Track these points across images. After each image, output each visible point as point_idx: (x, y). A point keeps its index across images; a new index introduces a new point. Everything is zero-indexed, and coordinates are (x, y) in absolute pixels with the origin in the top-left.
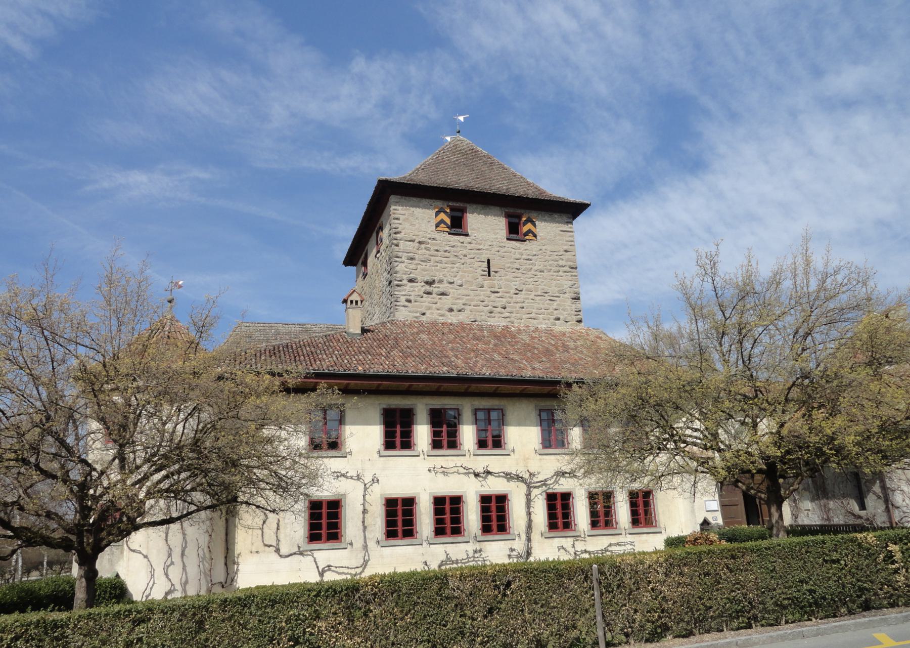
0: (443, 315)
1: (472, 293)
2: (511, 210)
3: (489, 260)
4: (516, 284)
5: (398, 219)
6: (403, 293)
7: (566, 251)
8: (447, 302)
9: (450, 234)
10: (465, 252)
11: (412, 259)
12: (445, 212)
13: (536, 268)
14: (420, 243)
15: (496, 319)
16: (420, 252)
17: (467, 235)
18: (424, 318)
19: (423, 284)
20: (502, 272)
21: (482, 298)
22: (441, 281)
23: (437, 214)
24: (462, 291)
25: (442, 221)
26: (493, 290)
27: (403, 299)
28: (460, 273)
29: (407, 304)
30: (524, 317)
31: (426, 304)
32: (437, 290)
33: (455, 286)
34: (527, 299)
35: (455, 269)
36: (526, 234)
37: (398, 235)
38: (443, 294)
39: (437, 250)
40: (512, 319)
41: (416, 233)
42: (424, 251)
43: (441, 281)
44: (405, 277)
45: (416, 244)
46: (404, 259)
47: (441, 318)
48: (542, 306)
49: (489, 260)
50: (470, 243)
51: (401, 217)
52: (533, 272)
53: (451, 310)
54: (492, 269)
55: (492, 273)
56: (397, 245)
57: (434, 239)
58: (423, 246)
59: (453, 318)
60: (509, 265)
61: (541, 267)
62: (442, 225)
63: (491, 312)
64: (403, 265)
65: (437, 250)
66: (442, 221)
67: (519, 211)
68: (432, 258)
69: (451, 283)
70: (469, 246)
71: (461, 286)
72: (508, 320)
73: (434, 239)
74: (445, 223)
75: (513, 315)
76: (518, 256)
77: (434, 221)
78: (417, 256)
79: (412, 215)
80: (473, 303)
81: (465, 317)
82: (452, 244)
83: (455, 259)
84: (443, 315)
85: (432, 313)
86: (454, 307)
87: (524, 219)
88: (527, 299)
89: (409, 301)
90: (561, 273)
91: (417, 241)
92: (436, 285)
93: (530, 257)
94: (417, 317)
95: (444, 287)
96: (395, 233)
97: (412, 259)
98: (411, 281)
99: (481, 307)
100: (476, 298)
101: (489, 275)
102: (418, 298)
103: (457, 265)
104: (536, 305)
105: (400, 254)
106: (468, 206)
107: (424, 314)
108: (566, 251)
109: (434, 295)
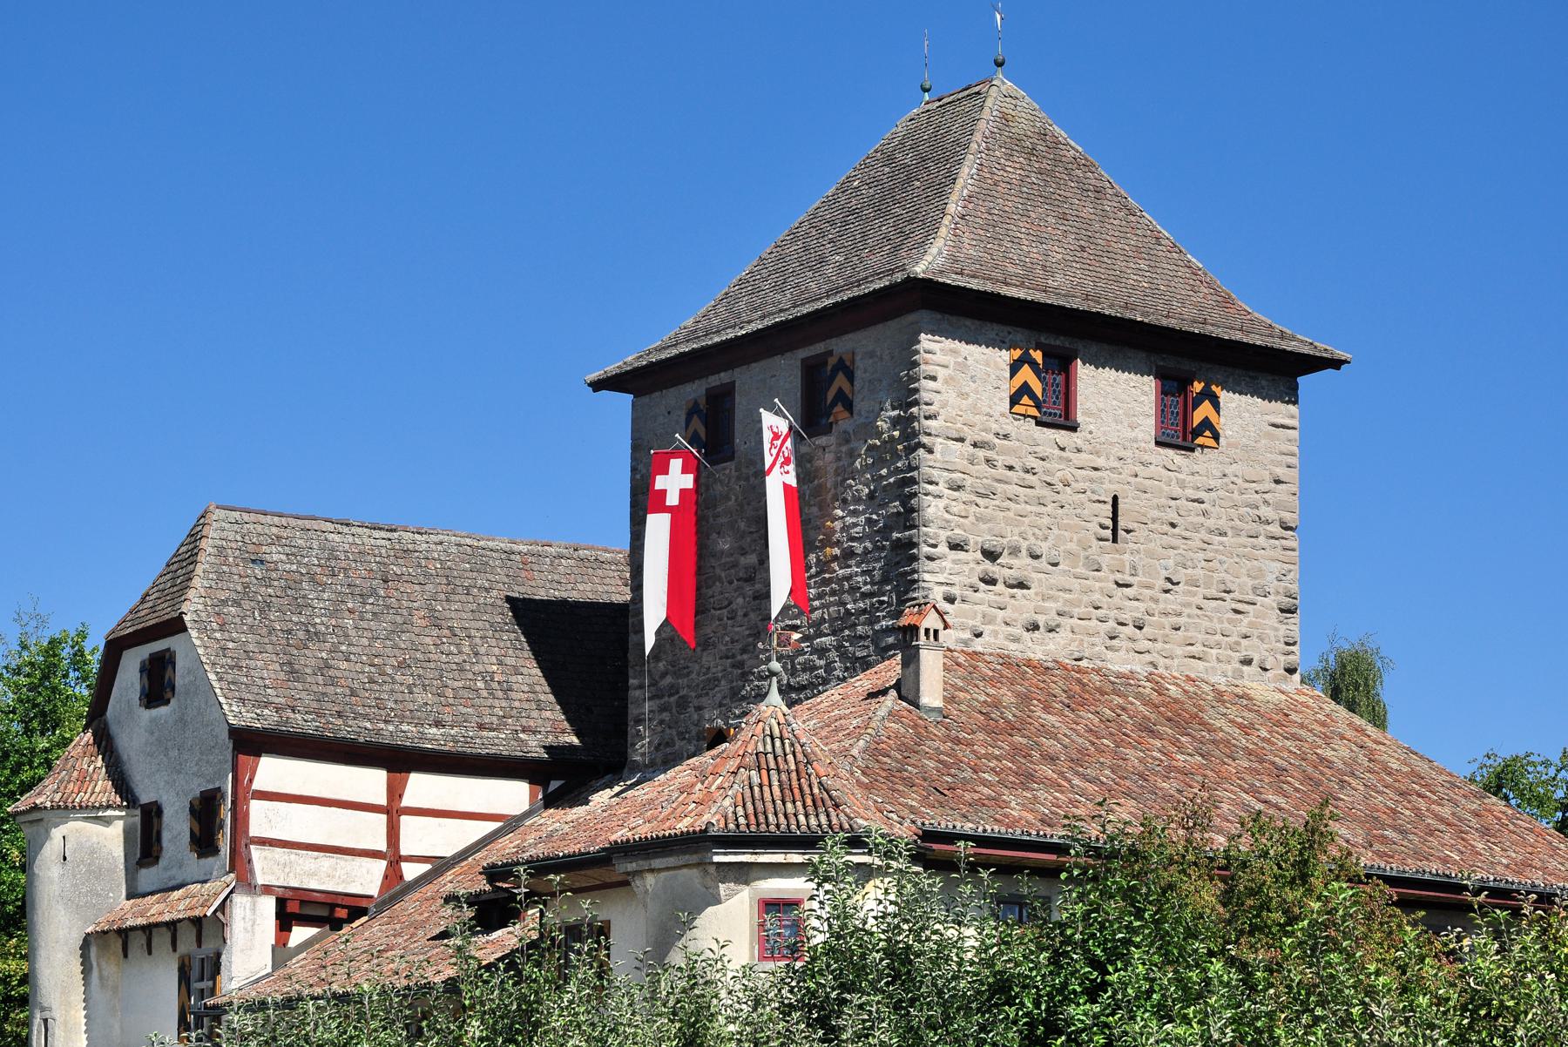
0: (1016, 640)
2: (1171, 363)
3: (1115, 498)
5: (934, 378)
8: (1024, 605)
9: (1039, 423)
12: (1033, 364)
13: (1211, 523)
17: (1074, 429)
18: (978, 646)
19: (979, 555)
20: (1141, 533)
23: (1015, 368)
24: (1057, 578)
25: (1025, 389)
26: (1118, 577)
28: (1056, 531)
31: (984, 608)
32: (1007, 572)
33: (1042, 564)
35: (1046, 521)
36: (1197, 432)
38: (1022, 585)
39: (1011, 468)
42: (984, 467)
43: (1015, 551)
49: (1115, 498)
51: (941, 373)
54: (1122, 523)
55: (1121, 533)
56: (931, 451)
57: (1006, 436)
58: (981, 453)
64: (941, 503)
65: (1011, 468)
66: (1025, 389)
67: (1187, 366)
68: (1000, 487)
69: (1036, 557)
71: (1055, 565)
73: (1006, 436)
74: (1032, 396)
76: (1177, 492)
77: (1007, 388)
78: (969, 481)
79: (962, 367)
80: (1076, 611)
94: (966, 643)
95: (1020, 566)
98: (955, 546)
99: (1094, 622)
100: (1085, 598)
101: (1115, 540)
102: (969, 593)
103: (1050, 508)
106: (1080, 345)
107: (978, 635)
109: (1000, 587)
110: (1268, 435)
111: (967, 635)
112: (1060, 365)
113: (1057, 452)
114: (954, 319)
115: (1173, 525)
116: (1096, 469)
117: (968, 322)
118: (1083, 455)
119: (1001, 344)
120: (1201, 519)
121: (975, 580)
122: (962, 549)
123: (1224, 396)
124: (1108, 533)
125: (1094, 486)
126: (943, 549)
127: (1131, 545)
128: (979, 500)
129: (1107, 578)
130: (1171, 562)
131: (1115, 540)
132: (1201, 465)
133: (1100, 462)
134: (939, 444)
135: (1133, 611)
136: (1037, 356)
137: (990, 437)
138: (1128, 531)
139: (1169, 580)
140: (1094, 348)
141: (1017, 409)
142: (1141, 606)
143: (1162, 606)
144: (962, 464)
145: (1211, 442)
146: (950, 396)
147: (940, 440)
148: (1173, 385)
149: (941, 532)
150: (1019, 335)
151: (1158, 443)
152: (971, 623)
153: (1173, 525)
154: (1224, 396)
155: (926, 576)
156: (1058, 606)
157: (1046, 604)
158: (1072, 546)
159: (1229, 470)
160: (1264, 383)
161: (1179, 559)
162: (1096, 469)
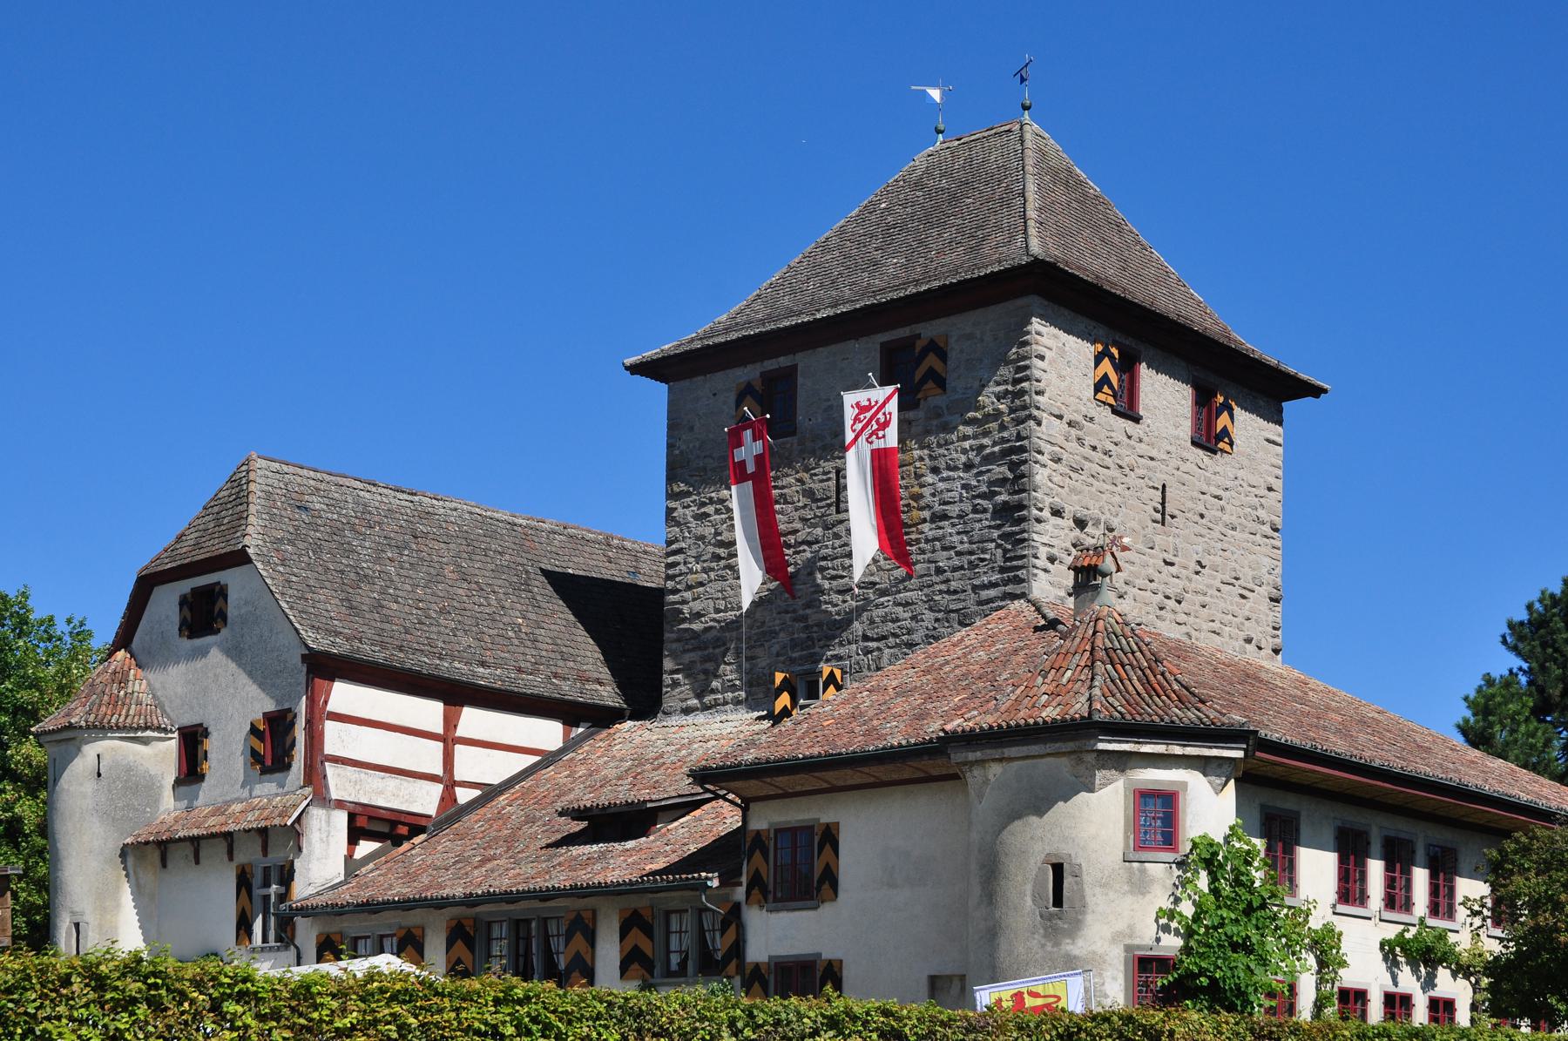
5: (1042, 358)
9: (1115, 412)
12: (1112, 357)
13: (1226, 518)
17: (1137, 419)
23: (1098, 360)
26: (1166, 556)
35: (1117, 499)
36: (1219, 438)
39: (1094, 448)
43: (1097, 523)
44: (1048, 500)
51: (1048, 354)
54: (1168, 510)
58: (1073, 432)
63: (1161, 609)
64: (1046, 472)
66: (1105, 380)
68: (1087, 465)
72: (1183, 629)
74: (1111, 387)
76: (1205, 488)
78: (1065, 456)
79: (1062, 352)
87: (1221, 399)
96: (1037, 393)
98: (1057, 513)
99: (1149, 594)
103: (1120, 488)
108: (1270, 489)
115: (1202, 516)
116: (1152, 459)
117: (1066, 312)
118: (1143, 445)
120: (1219, 514)
123: (1237, 411)
124: (1159, 516)
126: (1046, 514)
130: (1200, 549)
133: (1154, 453)
135: (1175, 587)
136: (1115, 351)
137: (1079, 418)
138: (1173, 517)
139: (1199, 563)
141: (1100, 396)
145: (1227, 448)
148: (1203, 399)
150: (1101, 331)
151: (1194, 443)
153: (1202, 516)
154: (1237, 411)
155: (1035, 537)
159: (1240, 474)
162: (1152, 459)
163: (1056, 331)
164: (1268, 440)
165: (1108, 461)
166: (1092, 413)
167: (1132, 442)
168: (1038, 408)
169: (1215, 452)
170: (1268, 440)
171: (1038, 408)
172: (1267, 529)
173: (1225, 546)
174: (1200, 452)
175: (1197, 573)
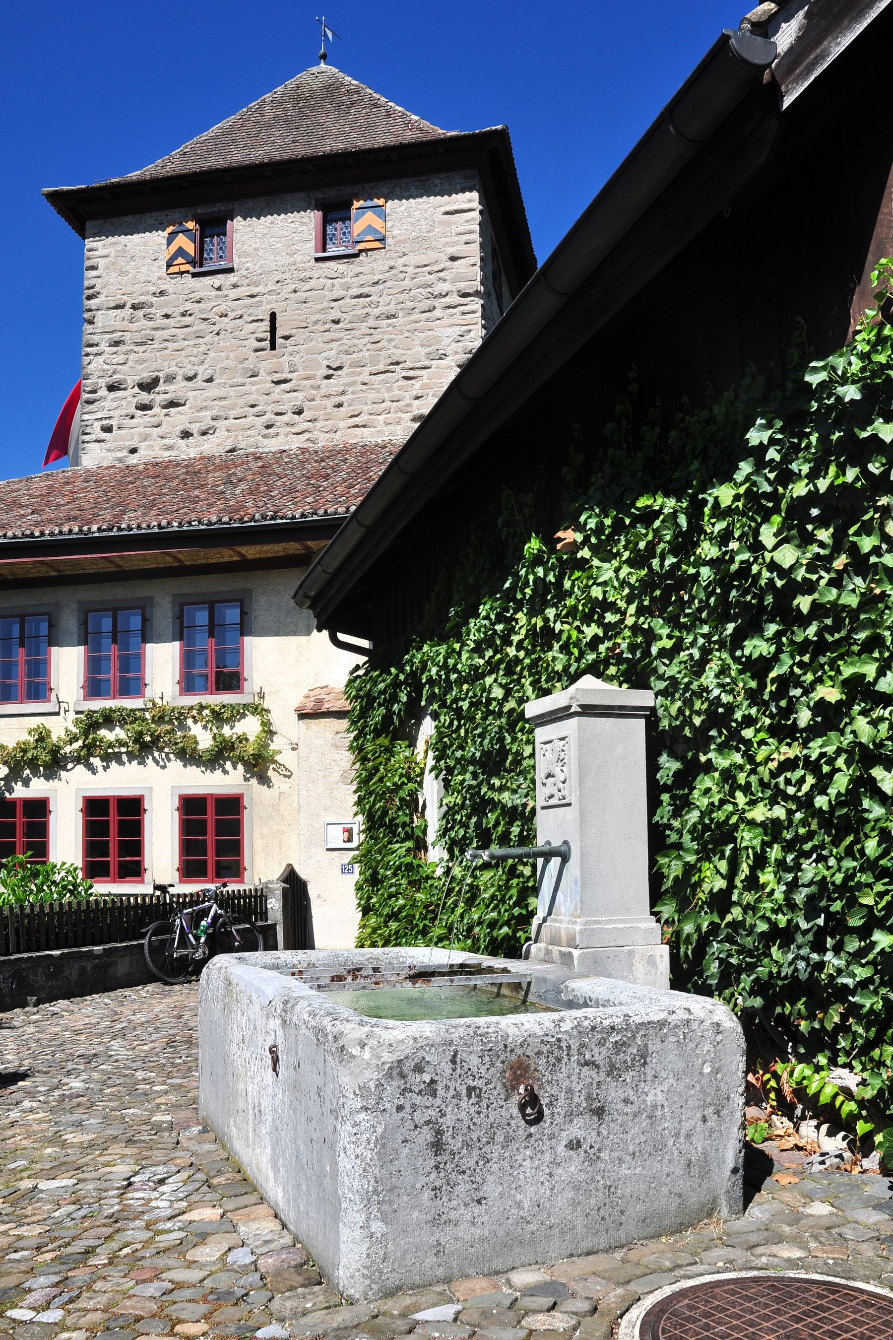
0: (169, 448)
1: (232, 392)
3: (273, 316)
4: (332, 355)
6: (99, 415)
7: (453, 259)
8: (179, 419)
9: (194, 275)
10: (223, 308)
11: (117, 343)
12: (186, 231)
14: (134, 307)
15: (281, 438)
16: (134, 327)
17: (231, 270)
18: (133, 460)
19: (136, 389)
20: (300, 336)
21: (251, 400)
22: (170, 379)
24: (213, 390)
25: (181, 252)
26: (277, 377)
27: (96, 431)
28: (212, 354)
29: (104, 435)
30: (342, 424)
33: (199, 382)
34: (353, 384)
35: (203, 348)
37: (92, 302)
39: (167, 316)
40: (316, 434)
41: (130, 289)
43: (170, 379)
44: (103, 382)
45: (127, 312)
46: (104, 347)
47: (166, 454)
48: (386, 396)
49: (273, 316)
50: (235, 286)
51: (102, 263)
52: (371, 322)
53: (186, 435)
54: (279, 333)
55: (279, 341)
56: (91, 322)
57: (162, 293)
58: (140, 313)
59: (189, 451)
60: (318, 317)
61: (392, 309)
62: (180, 260)
63: (268, 427)
64: (100, 359)
65: (167, 316)
66: (181, 252)
68: (158, 334)
70: (234, 293)
72: (307, 436)
73: (162, 293)
75: (318, 425)
78: (127, 336)
80: (232, 414)
81: (212, 446)
82: (196, 296)
83: (203, 326)
84: (169, 448)
85: (151, 447)
86: (195, 428)
88: (353, 384)
89: (108, 429)
90: (437, 313)
91: (129, 305)
92: (161, 387)
93: (365, 290)
94: (120, 460)
96: (89, 298)
97: (117, 343)
98: (112, 388)
100: (241, 402)
101: (273, 347)
104: (372, 396)
105: (96, 339)
107: (133, 451)
108: (453, 259)
109: (157, 410)
110: (442, 223)
111: (125, 453)
112: (213, 227)
113: (215, 293)
114: (115, 220)
115: (336, 322)
116: (252, 296)
117: (129, 218)
119: (161, 227)
121: (132, 410)
122: (119, 389)
125: (250, 311)
126: (103, 392)
127: (290, 349)
128: (136, 349)
129: (264, 381)
131: (273, 347)
132: (371, 266)
133: (254, 290)
134: (100, 316)
140: (250, 203)
141: (173, 269)
142: (300, 395)
143: (323, 391)
144: (126, 325)
146: (113, 277)
147: (100, 312)
148: (335, 212)
149: (100, 380)
150: (177, 215)
152: (127, 443)
156: (214, 412)
157: (202, 414)
158: (230, 363)
160: (437, 182)
161: (342, 348)
162: (252, 296)
163: (116, 239)
164: (447, 213)
165: (187, 320)
166: (163, 287)
167: (225, 292)
168: (90, 310)
169: (356, 256)
170: (447, 213)
171: (90, 310)
172: (454, 299)
173: (375, 338)
174: (332, 264)
175: (328, 377)
